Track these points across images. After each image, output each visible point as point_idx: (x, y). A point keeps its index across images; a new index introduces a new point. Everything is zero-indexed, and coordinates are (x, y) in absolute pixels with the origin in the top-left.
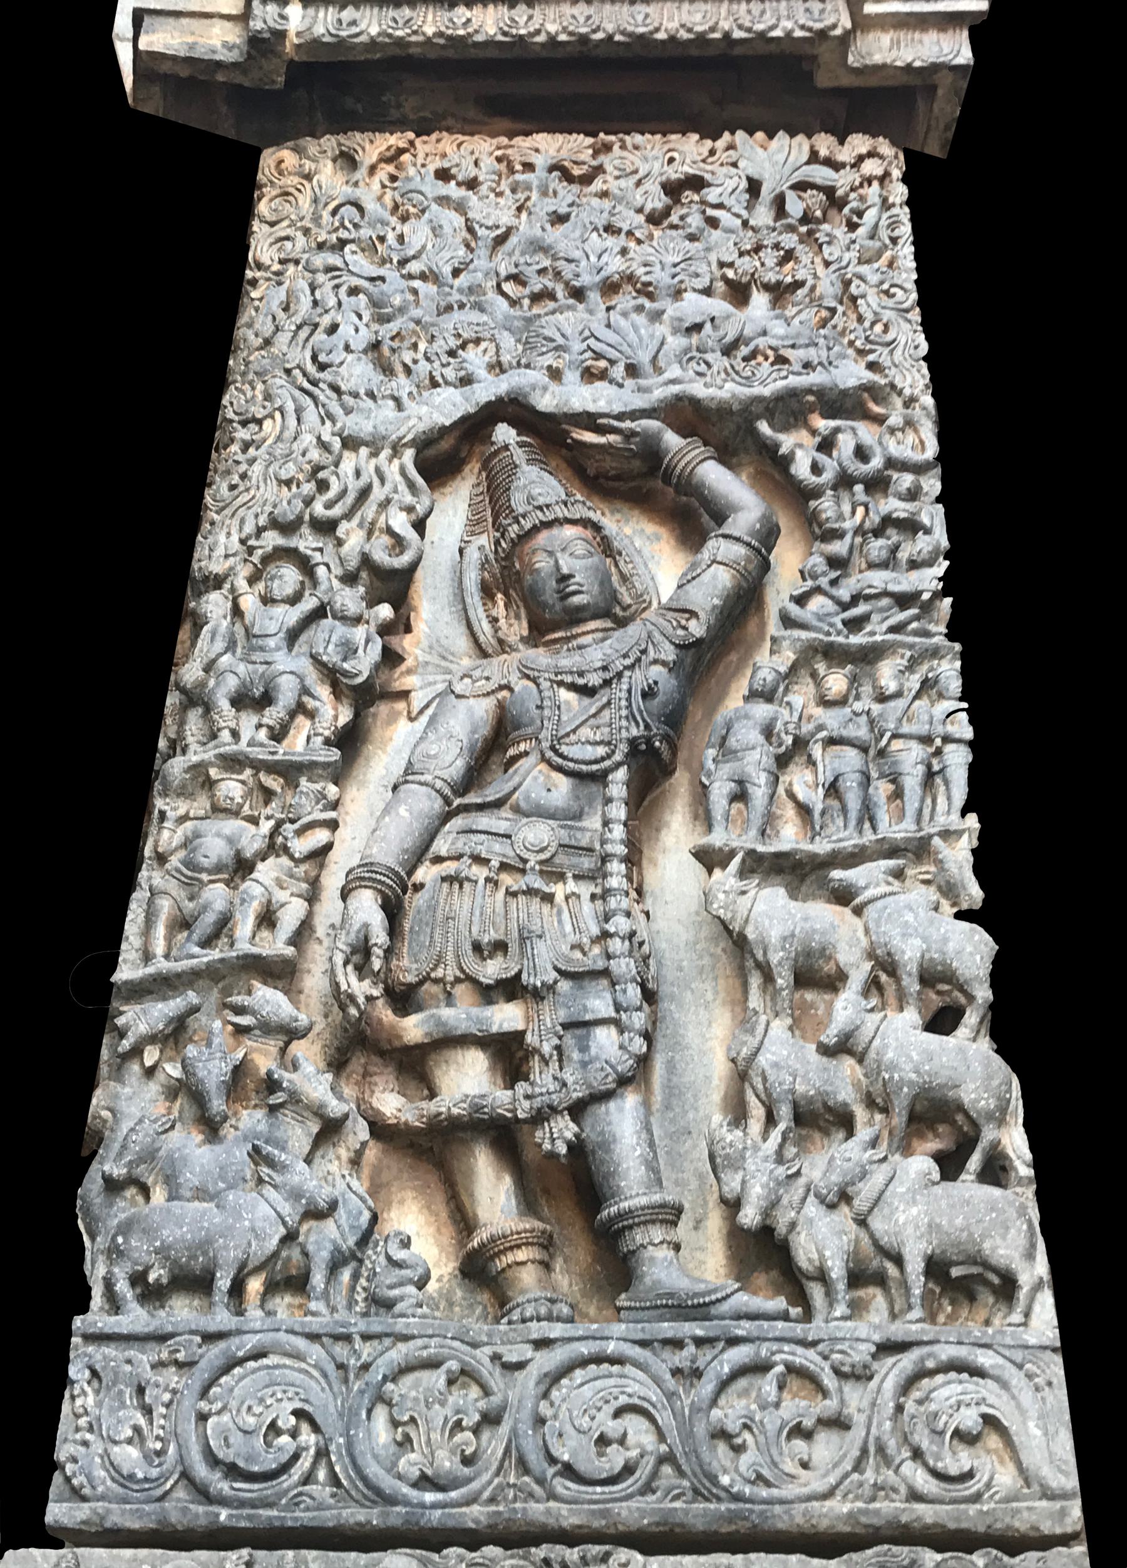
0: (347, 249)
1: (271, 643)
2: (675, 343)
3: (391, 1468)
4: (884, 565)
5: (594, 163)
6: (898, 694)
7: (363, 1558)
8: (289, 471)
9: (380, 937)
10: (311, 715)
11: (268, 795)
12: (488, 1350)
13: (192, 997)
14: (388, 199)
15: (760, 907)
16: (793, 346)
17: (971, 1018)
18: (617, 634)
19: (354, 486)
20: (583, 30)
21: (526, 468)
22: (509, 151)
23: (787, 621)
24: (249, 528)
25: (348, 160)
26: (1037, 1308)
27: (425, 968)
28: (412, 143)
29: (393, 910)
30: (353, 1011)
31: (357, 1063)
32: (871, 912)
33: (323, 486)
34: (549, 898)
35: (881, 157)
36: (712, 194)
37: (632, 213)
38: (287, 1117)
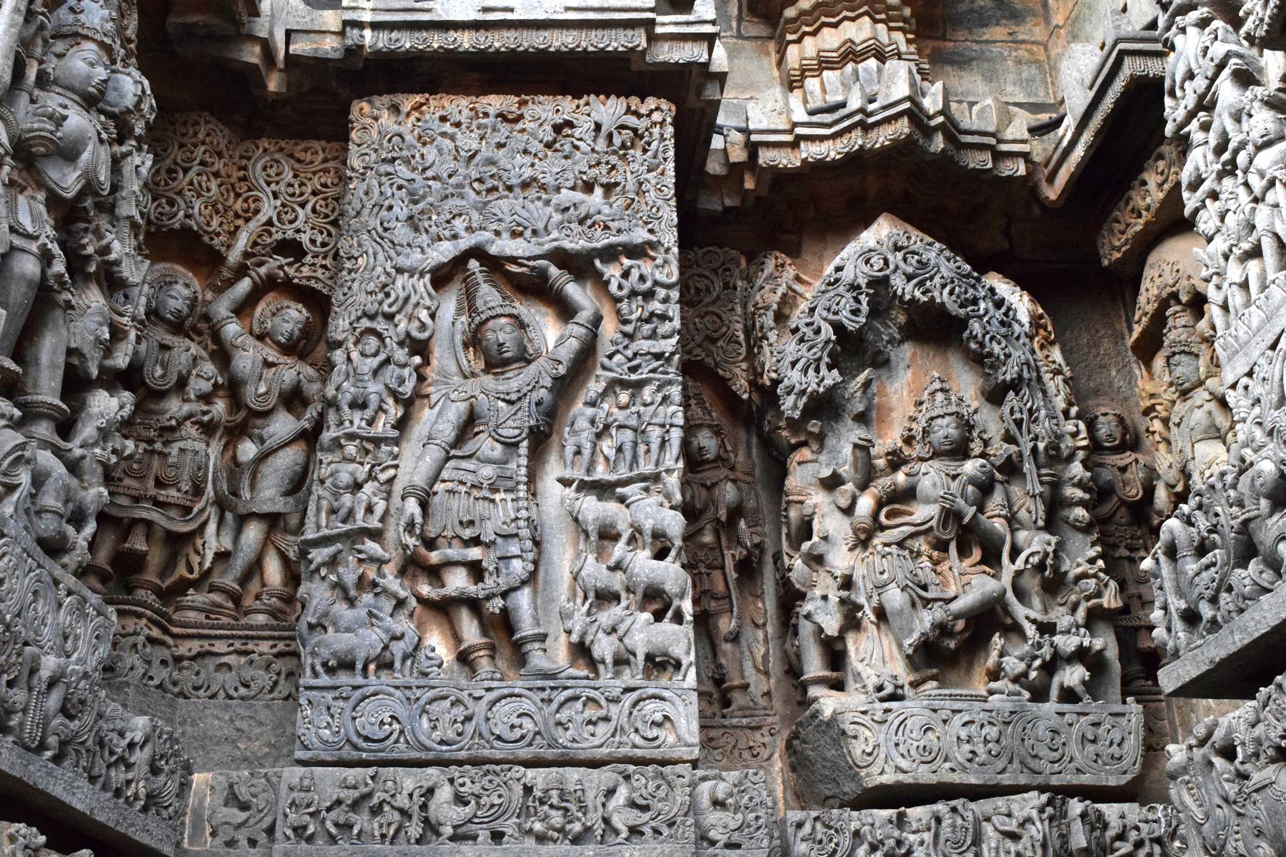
1: (366, 378)
2: (557, 217)
3: (429, 738)
6: (652, 403)
7: (419, 770)
8: (371, 287)
9: (419, 520)
10: (385, 412)
11: (367, 452)
13: (339, 546)
15: (584, 506)
17: (673, 553)
18: (525, 370)
19: (402, 295)
21: (484, 285)
23: (604, 368)
24: (353, 318)
25: (395, 109)
27: (439, 531)
29: (424, 505)
31: (410, 571)
32: (632, 507)
33: (387, 295)
36: (577, 133)
37: (537, 143)
38: (383, 598)
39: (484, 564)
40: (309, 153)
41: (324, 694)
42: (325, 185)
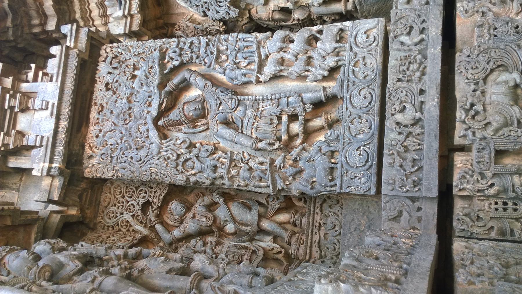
0: (112, 155)
2: (145, 88)
4: (199, 49)
5: (99, 105)
6: (227, 46)
8: (164, 165)
10: (219, 158)
12: (347, 118)
14: (101, 148)
15: (268, 71)
16: (149, 65)
20: (69, 104)
22: (93, 123)
23: (210, 66)
24: (177, 173)
25: (90, 157)
26: (346, 25)
27: (273, 135)
28: (88, 144)
29: (261, 141)
30: (282, 146)
32: (271, 52)
33: (169, 158)
34: (262, 111)
35: (106, 48)
37: (113, 97)
39: (290, 113)
40: (106, 200)
41: (344, 181)
42: (121, 192)
